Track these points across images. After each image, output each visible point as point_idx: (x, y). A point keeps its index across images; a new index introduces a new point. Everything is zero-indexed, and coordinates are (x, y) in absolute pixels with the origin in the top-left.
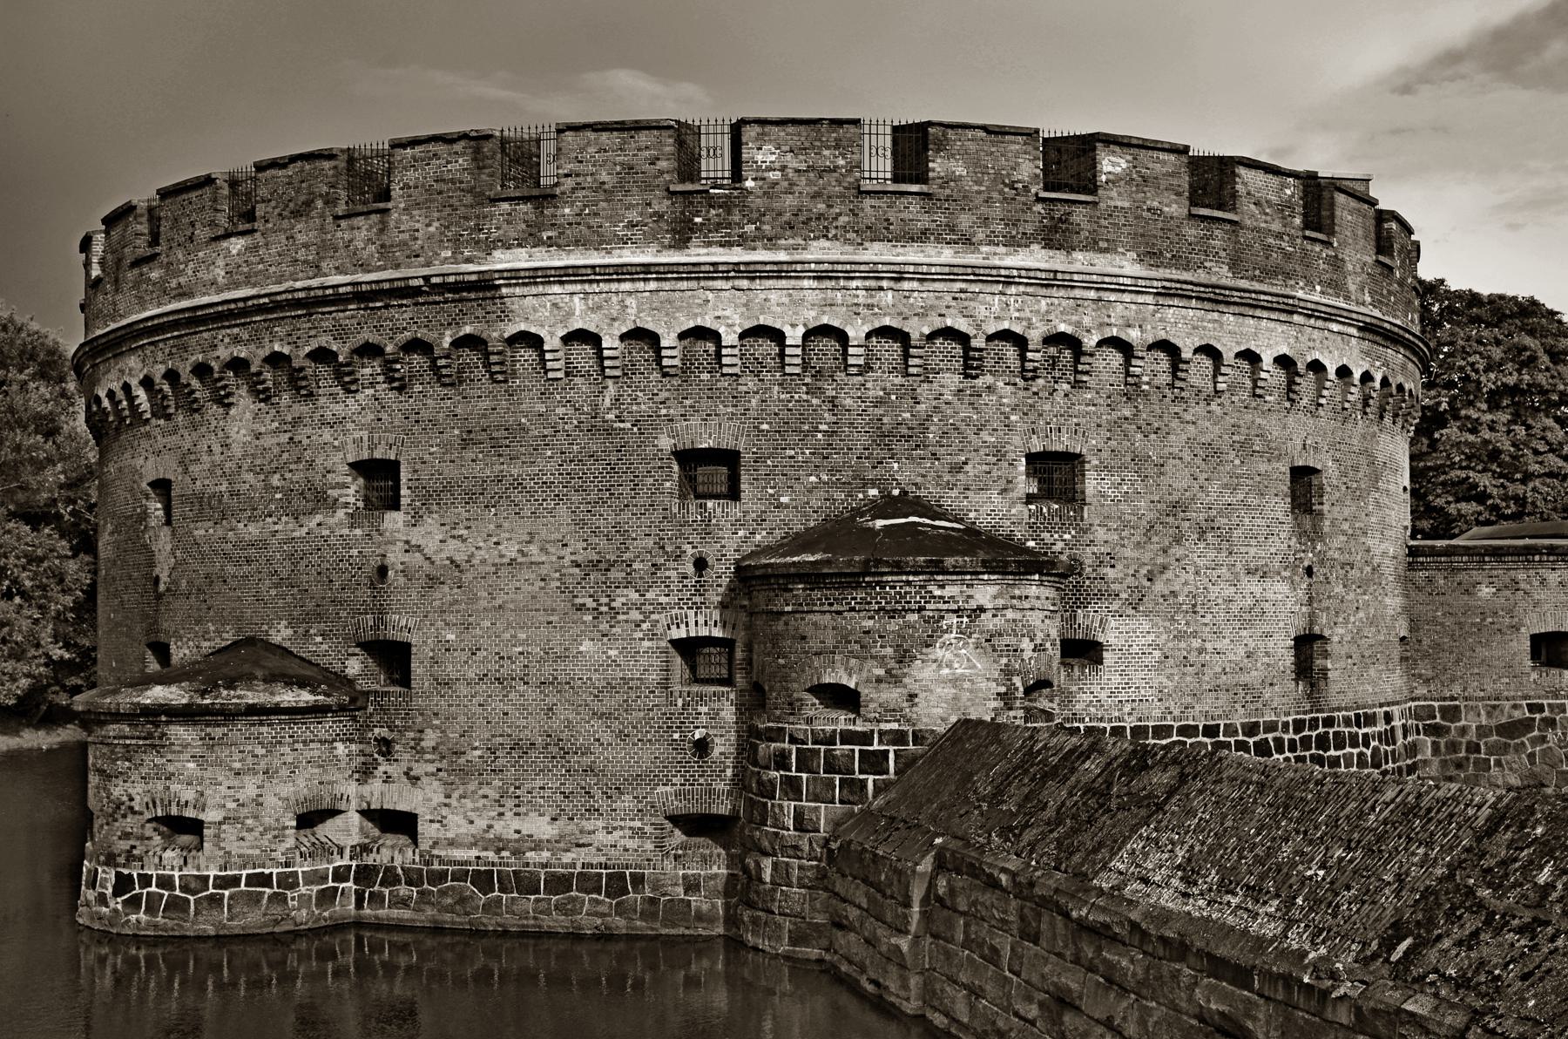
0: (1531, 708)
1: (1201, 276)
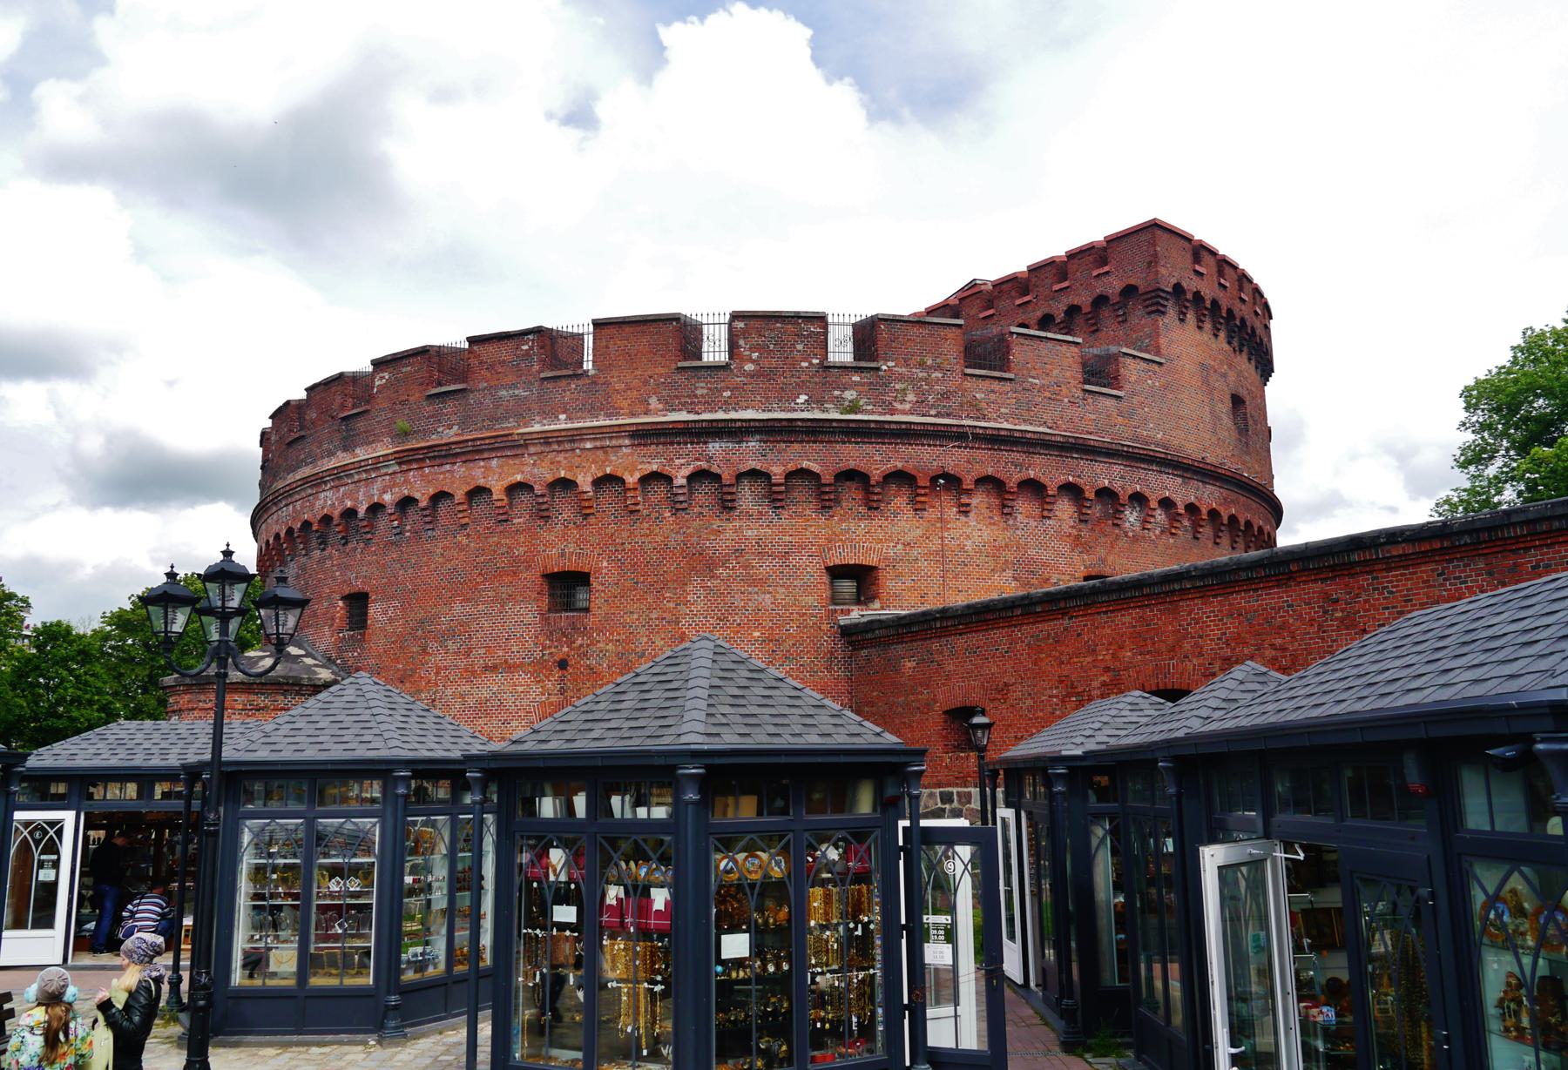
1: (434, 440)
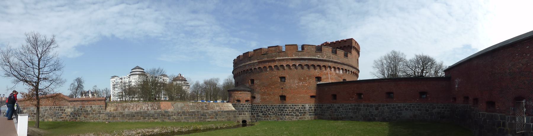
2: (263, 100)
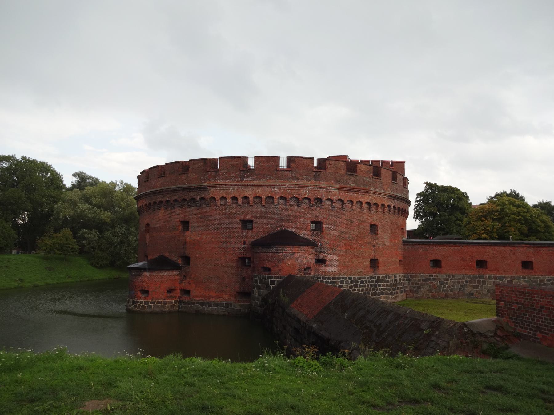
0: (430, 276)
2: (343, 266)
